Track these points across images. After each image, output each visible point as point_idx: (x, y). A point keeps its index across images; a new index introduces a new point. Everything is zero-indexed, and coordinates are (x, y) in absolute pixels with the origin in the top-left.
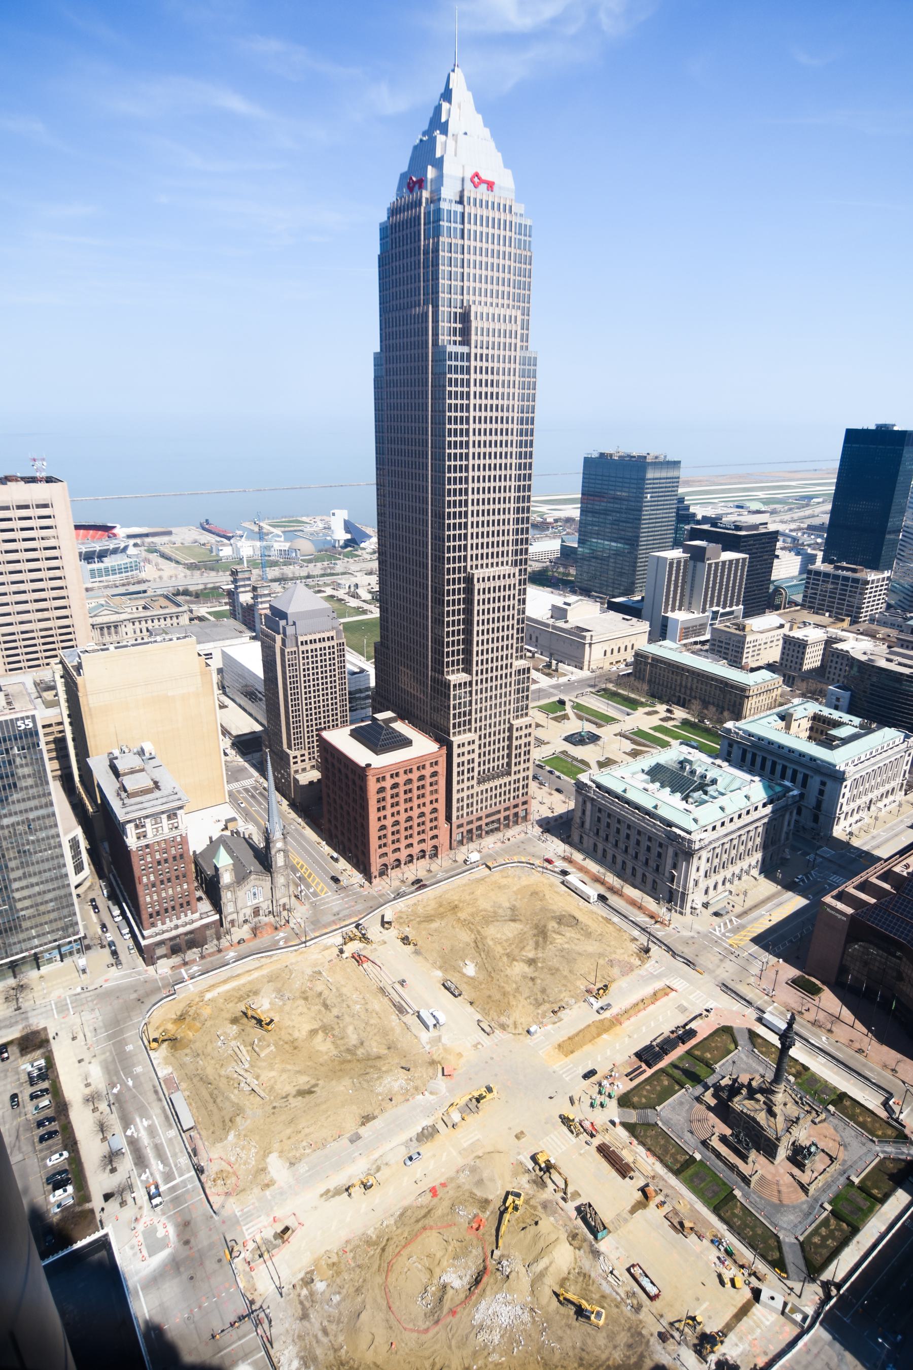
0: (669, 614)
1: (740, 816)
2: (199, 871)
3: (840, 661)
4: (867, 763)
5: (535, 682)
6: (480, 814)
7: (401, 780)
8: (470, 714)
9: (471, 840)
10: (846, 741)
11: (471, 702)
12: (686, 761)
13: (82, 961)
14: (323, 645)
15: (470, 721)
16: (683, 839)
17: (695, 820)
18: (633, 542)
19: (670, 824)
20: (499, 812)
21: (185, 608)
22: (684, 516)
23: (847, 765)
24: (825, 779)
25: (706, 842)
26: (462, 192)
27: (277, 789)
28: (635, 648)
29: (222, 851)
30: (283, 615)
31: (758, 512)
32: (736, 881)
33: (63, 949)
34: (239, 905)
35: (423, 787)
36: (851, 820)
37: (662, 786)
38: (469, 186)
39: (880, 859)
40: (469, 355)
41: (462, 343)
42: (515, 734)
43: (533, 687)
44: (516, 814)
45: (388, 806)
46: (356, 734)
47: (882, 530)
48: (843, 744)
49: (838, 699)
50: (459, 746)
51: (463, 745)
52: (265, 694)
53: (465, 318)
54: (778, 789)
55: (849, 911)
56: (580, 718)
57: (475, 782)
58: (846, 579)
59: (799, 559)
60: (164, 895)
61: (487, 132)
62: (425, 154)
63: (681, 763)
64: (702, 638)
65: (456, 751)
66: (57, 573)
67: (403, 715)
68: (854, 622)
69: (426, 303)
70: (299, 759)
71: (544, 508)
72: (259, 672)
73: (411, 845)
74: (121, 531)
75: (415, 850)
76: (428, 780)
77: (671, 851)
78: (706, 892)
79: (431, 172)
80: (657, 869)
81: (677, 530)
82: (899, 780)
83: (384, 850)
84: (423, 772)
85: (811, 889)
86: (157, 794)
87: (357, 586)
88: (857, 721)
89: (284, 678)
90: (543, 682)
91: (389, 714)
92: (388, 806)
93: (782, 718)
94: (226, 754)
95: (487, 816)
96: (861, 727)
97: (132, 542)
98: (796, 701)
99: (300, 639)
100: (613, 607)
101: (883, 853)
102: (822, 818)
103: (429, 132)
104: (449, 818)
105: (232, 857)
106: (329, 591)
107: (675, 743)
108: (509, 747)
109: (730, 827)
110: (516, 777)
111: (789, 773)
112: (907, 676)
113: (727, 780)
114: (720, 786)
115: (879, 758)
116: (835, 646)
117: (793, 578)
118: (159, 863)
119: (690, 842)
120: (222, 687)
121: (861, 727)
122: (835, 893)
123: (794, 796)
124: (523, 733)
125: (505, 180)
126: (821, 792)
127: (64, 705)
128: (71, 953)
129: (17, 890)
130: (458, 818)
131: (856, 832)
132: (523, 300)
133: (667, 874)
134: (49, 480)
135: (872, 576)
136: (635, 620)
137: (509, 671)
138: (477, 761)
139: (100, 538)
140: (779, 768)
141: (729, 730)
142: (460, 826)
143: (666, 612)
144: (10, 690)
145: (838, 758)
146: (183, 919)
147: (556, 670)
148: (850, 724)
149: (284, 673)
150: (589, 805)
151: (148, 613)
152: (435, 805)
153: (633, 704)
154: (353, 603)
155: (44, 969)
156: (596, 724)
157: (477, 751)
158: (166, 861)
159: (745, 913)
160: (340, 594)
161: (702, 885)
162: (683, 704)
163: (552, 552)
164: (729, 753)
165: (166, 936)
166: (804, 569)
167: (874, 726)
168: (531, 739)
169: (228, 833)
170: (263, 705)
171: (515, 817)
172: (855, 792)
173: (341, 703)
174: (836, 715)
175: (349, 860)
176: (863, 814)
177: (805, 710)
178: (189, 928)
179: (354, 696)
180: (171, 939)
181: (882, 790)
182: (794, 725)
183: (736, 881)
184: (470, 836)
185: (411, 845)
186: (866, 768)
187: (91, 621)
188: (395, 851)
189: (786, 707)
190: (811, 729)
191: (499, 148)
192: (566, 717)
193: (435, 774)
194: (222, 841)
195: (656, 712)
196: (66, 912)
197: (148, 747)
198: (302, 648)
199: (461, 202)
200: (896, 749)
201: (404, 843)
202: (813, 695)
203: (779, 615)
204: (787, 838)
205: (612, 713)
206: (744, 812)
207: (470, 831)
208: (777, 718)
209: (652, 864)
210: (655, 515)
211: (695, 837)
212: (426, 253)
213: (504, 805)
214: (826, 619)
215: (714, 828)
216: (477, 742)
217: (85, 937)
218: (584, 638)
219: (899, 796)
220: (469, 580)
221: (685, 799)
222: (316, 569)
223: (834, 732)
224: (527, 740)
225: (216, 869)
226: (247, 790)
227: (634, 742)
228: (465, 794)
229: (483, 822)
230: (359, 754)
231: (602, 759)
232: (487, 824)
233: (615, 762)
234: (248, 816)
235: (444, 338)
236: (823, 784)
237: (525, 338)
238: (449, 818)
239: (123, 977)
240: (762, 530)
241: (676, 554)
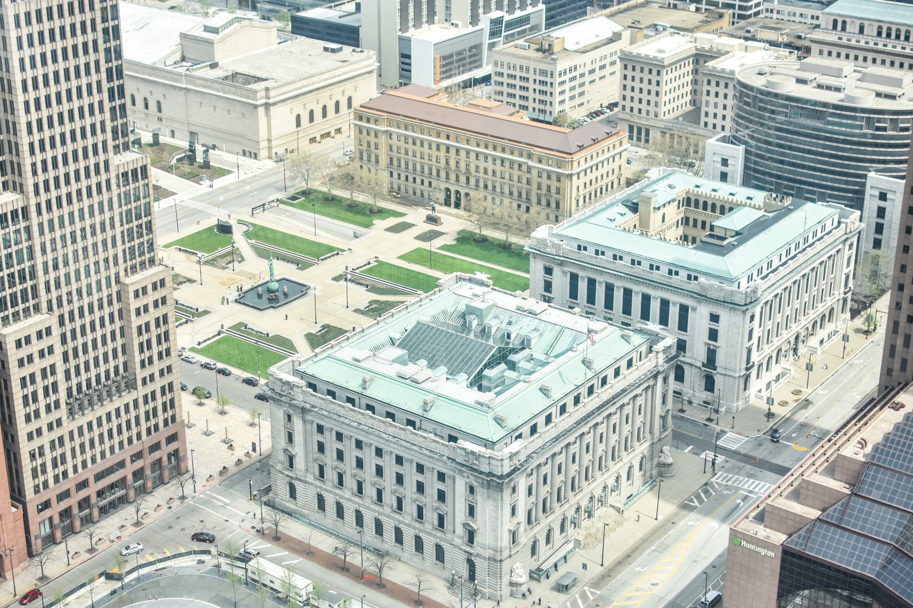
0: (412, 33)
1: (577, 400)
3: (722, 90)
4: (782, 271)
6: (83, 475)
8: (33, 275)
9: (70, 531)
10: (743, 236)
11: (31, 249)
12: (470, 310)
15: (34, 288)
17: (499, 421)
20: (122, 464)
23: (750, 278)
24: (717, 310)
25: (522, 458)
28: (356, 104)
32: (586, 523)
36: (768, 376)
37: (432, 365)
42: (134, 304)
48: (741, 243)
49: (725, 162)
50: (19, 344)
51: (28, 340)
54: (637, 339)
56: (262, 254)
57: (63, 412)
63: (463, 316)
64: (478, 74)
77: (461, 486)
78: (534, 551)
80: (441, 524)
82: (839, 293)
88: (760, 196)
90: (183, 191)
93: (634, 208)
95: (99, 477)
96: (767, 208)
98: (654, 173)
100: (302, 27)
102: (719, 381)
107: (444, 278)
109: (562, 423)
110: (148, 389)
111: (655, 307)
112: (836, 107)
113: (549, 337)
114: (537, 350)
115: (801, 258)
116: (711, 64)
123: (667, 349)
124: (149, 299)
126: (713, 335)
130: (37, 490)
133: (460, 530)
136: (347, 49)
137: (103, 177)
138: (60, 368)
140: (637, 302)
141: (543, 242)
143: (404, 27)
147: (206, 165)
148: (750, 204)
150: (298, 423)
153: (364, 214)
156: (296, 262)
157: (59, 350)
159: (607, 576)
161: (524, 539)
162: (454, 200)
164: (548, 286)
167: (788, 201)
168: (168, 309)
172: (769, 325)
174: (724, 191)
176: (786, 363)
177: (669, 186)
181: (813, 315)
182: (655, 218)
183: (586, 523)
186: (782, 279)
189: (637, 186)
190: (686, 221)
195: (405, 226)
200: (828, 239)
202: (686, 157)
203: (611, 16)
204: (664, 427)
205: (324, 238)
206: (584, 391)
207: (66, 513)
208: (625, 210)
209: (431, 517)
214: (689, 15)
215: (534, 430)
216: (56, 331)
219: (843, 322)
221: (478, 383)
223: (724, 222)
224: (160, 313)
228: (45, 440)
229: (91, 491)
231: (315, 329)
232: (100, 494)
233: (340, 332)
236: (715, 318)
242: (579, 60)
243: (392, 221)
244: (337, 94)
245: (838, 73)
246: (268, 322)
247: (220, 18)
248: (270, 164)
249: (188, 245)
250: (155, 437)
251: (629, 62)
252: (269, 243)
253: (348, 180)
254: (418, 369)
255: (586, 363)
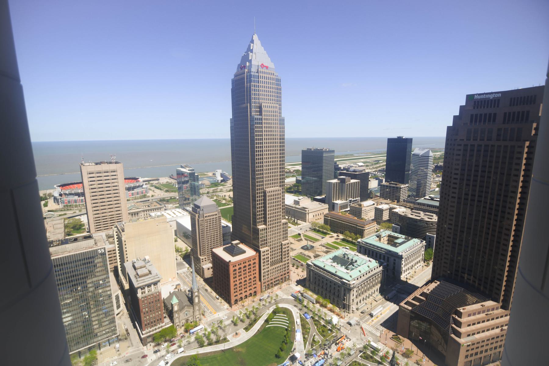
0: (335, 202)
2: (165, 306)
5: (289, 227)
6: (272, 278)
7: (242, 266)
9: (269, 288)
10: (401, 244)
12: (345, 254)
13: (117, 345)
14: (213, 217)
16: (347, 283)
17: (351, 276)
18: (320, 177)
19: (342, 278)
21: (163, 206)
22: (337, 168)
26: (258, 69)
27: (196, 272)
29: (174, 297)
30: (198, 207)
31: (362, 166)
32: (368, 299)
33: (110, 341)
34: (181, 319)
35: (250, 268)
36: (406, 273)
38: (260, 67)
39: (418, 288)
40: (262, 119)
41: (259, 115)
42: (283, 247)
43: (289, 229)
44: (285, 277)
45: (238, 276)
46: (225, 250)
47: (404, 171)
52: (189, 236)
53: (260, 107)
55: (410, 308)
56: (306, 239)
58: (394, 187)
59: (377, 181)
60: (151, 316)
61: (265, 52)
62: (246, 58)
64: (347, 210)
65: (262, 254)
66: (117, 195)
67: (242, 242)
68: (398, 201)
69: (247, 103)
70: (204, 260)
71: (289, 167)
72: (190, 228)
73: (246, 291)
74: (141, 180)
75: (248, 293)
76: (252, 266)
77: (343, 289)
79: (248, 64)
81: (335, 173)
82: (421, 257)
83: (236, 294)
84: (250, 263)
85: (395, 300)
86: (150, 276)
87: (225, 196)
88: (404, 236)
89: (199, 230)
91: (237, 241)
92: (238, 276)
93: (378, 237)
94: (177, 259)
96: (405, 239)
97: (145, 183)
98: (382, 230)
99: (205, 215)
101: (419, 285)
103: (247, 52)
104: (260, 280)
105: (178, 300)
106: (215, 198)
107: (340, 247)
108: (281, 252)
109: (363, 278)
113: (361, 260)
114: (358, 263)
117: (375, 188)
118: (150, 303)
119: (349, 285)
120: (176, 235)
121: (405, 239)
122: (404, 302)
125: (271, 65)
127: (116, 243)
128: (113, 342)
129: (94, 317)
131: (409, 278)
132: (279, 100)
134: (116, 163)
135: (402, 186)
138: (270, 257)
139: (133, 182)
142: (264, 283)
144: (97, 238)
145: (399, 250)
146: (159, 326)
148: (401, 238)
149: (199, 228)
150: (311, 272)
151: (150, 208)
152: (255, 275)
153: (325, 234)
154: (224, 202)
155: (102, 350)
158: (152, 302)
160: (219, 199)
161: (355, 301)
163: (293, 182)
165: (151, 333)
166: (379, 185)
168: (289, 248)
169: (177, 290)
170: (191, 240)
171: (285, 278)
173: (220, 238)
174: (396, 235)
175: (223, 298)
176: (410, 271)
177: (385, 233)
178: (161, 329)
179: (224, 235)
180: (153, 335)
181: (416, 261)
182: (382, 239)
183: (368, 299)
184: (268, 287)
185: (246, 291)
187: (129, 212)
188: (240, 294)
190: (388, 240)
191: (269, 56)
192: (301, 240)
193: (254, 263)
194: (174, 293)
196: (112, 325)
197: (147, 258)
198: (205, 219)
199: (258, 72)
201: (244, 290)
207: (268, 285)
209: (336, 294)
210: (327, 168)
211: (351, 283)
212: (247, 88)
213: (280, 274)
214: (388, 201)
217: (119, 335)
218: (306, 211)
220: (265, 192)
221: (347, 268)
222: (211, 190)
223: (396, 241)
225: (172, 305)
226: (184, 273)
227: (327, 248)
229: (273, 281)
230: (226, 257)
234: (184, 283)
235: (253, 114)
236: (395, 260)
237: (280, 113)
238: (260, 280)
239: (133, 351)
240: (364, 172)
241: (335, 181)
242: (367, 208)
243: (330, 236)
244: (321, 212)
245: (419, 213)
246: (307, 253)
247: (301, 197)
248: (308, 223)
249: (294, 237)
250: (285, 272)
251: (377, 210)
252: (308, 238)
253: (322, 227)
254: (335, 264)
255: (368, 267)
